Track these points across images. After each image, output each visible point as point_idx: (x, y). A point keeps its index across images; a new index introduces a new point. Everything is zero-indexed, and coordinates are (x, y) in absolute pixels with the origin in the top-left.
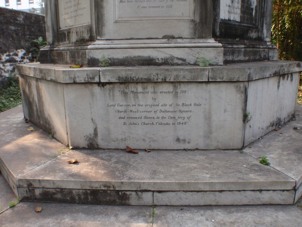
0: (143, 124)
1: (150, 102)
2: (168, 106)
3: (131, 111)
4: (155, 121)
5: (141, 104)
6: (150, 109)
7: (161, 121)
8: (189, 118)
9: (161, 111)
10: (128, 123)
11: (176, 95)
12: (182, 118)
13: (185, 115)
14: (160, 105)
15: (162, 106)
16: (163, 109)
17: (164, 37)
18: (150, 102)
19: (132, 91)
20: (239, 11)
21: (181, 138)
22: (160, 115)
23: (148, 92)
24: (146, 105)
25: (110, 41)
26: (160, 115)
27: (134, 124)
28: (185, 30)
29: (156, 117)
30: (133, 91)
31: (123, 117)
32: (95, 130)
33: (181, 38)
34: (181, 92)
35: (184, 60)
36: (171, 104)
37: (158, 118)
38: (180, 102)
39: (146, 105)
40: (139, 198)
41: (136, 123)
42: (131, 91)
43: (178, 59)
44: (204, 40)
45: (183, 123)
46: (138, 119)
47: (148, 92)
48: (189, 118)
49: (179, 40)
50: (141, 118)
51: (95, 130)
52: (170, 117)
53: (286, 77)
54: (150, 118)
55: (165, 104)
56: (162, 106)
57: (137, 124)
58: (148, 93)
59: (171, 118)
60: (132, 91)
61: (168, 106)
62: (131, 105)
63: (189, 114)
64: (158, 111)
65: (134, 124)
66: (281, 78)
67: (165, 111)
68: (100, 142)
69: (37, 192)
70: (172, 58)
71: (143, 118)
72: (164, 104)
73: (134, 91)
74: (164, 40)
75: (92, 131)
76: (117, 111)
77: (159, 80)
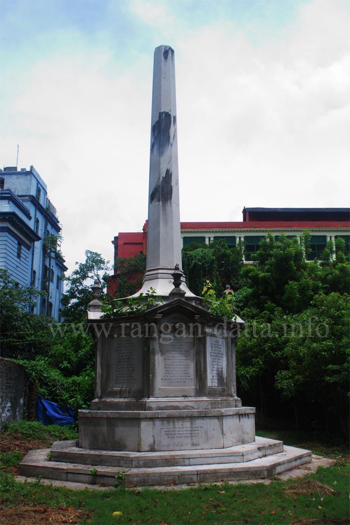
1: (180, 426)
4: (182, 436)
6: (179, 429)
7: (185, 435)
8: (198, 433)
11: (192, 423)
13: (196, 432)
17: (182, 397)
18: (180, 426)
20: (216, 381)
21: (195, 443)
22: (185, 432)
25: (156, 399)
26: (185, 432)
27: (173, 437)
28: (193, 393)
32: (154, 441)
33: (190, 397)
35: (193, 407)
38: (194, 426)
40: (184, 462)
43: (190, 407)
44: (201, 398)
48: (198, 433)
49: (190, 398)
51: (154, 441)
53: (244, 416)
63: (198, 432)
65: (173, 437)
66: (241, 416)
68: (156, 448)
69: (141, 463)
70: (187, 406)
74: (183, 398)
75: (152, 441)
77: (185, 416)
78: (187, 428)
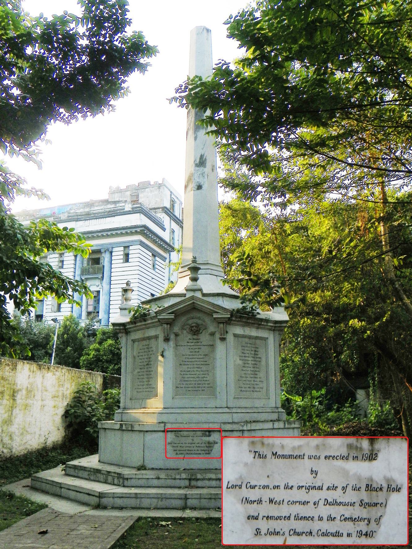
0: (292, 532)
2: (339, 490)
3: (271, 501)
5: (290, 485)
9: (327, 503)
10: (264, 531)
12: (366, 521)
14: (325, 488)
15: (328, 489)
16: (331, 496)
19: (274, 453)
23: (304, 455)
24: (300, 487)
29: (316, 518)
30: (276, 453)
31: (256, 514)
34: (364, 458)
36: (345, 486)
37: (321, 519)
39: (300, 487)
41: (280, 531)
42: (273, 452)
45: (368, 533)
46: (283, 520)
47: (304, 455)
50: (289, 518)
52: (343, 518)
54: (305, 518)
55: (335, 486)
56: (328, 489)
57: (281, 533)
58: (303, 458)
59: (344, 519)
60: (274, 453)
61: (339, 489)
62: (271, 487)
64: (322, 503)
67: (335, 503)
71: (292, 518)
72: (332, 486)
73: (278, 454)
76: (244, 499)
78: (335, 488)
